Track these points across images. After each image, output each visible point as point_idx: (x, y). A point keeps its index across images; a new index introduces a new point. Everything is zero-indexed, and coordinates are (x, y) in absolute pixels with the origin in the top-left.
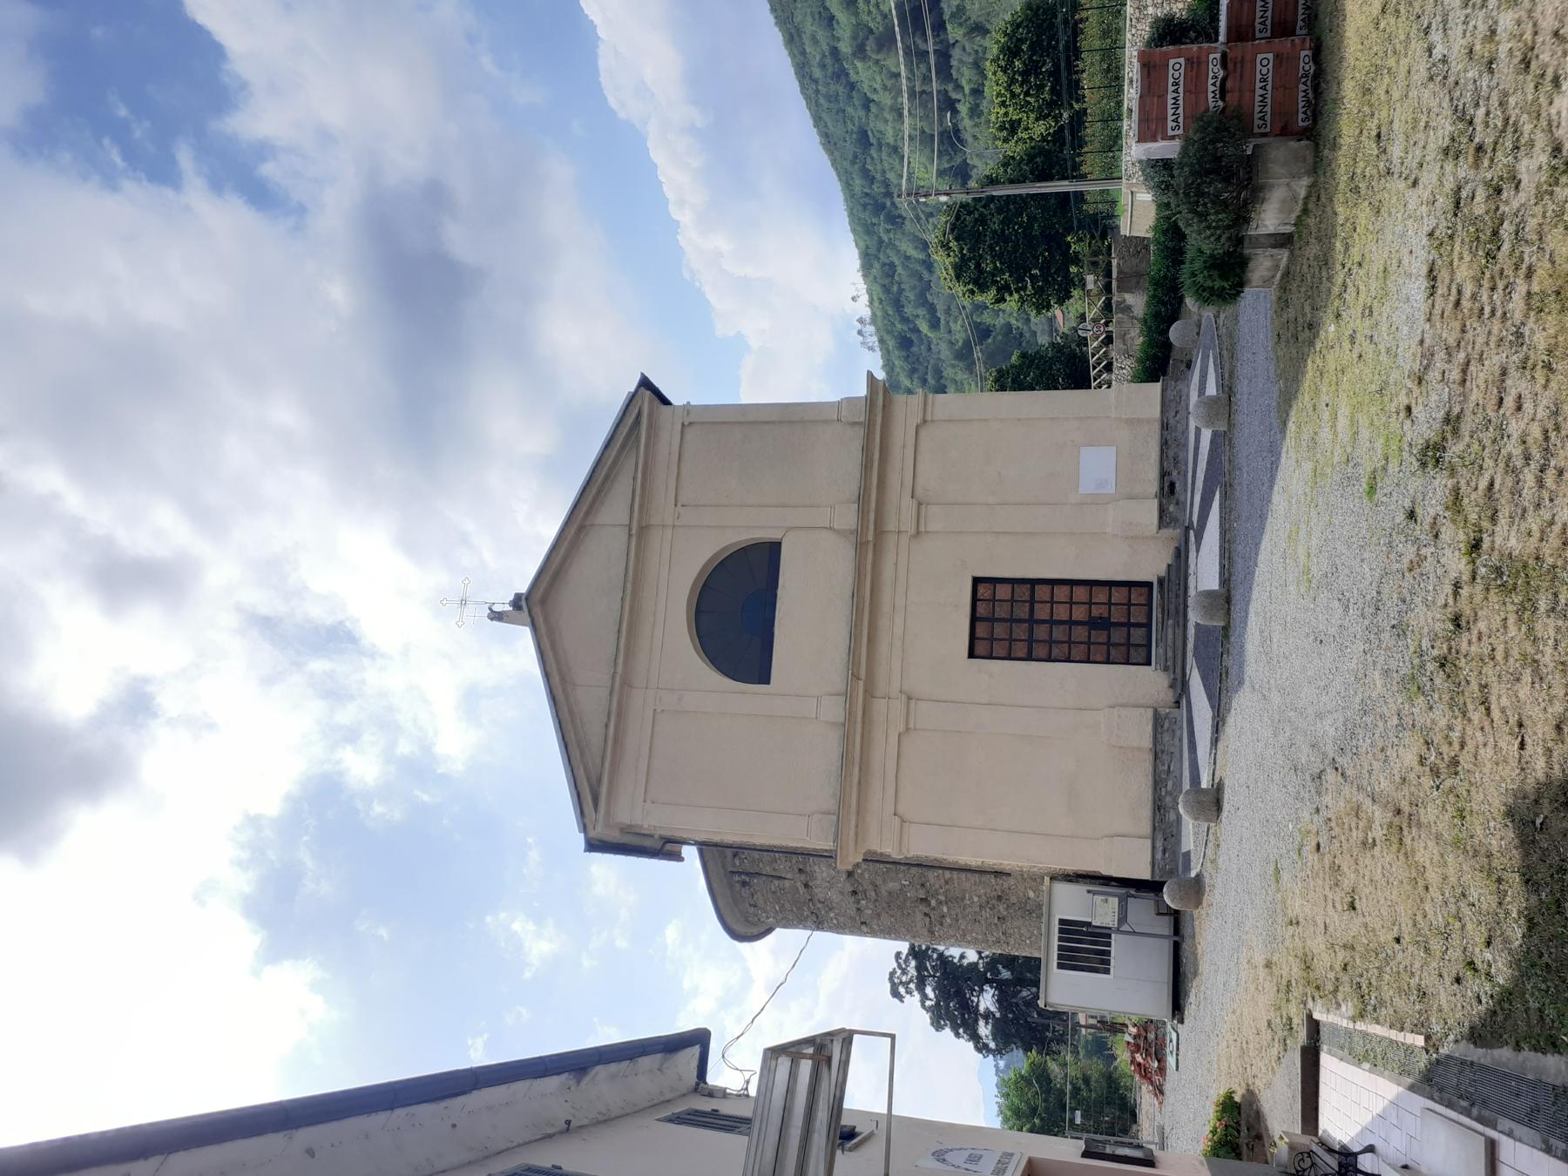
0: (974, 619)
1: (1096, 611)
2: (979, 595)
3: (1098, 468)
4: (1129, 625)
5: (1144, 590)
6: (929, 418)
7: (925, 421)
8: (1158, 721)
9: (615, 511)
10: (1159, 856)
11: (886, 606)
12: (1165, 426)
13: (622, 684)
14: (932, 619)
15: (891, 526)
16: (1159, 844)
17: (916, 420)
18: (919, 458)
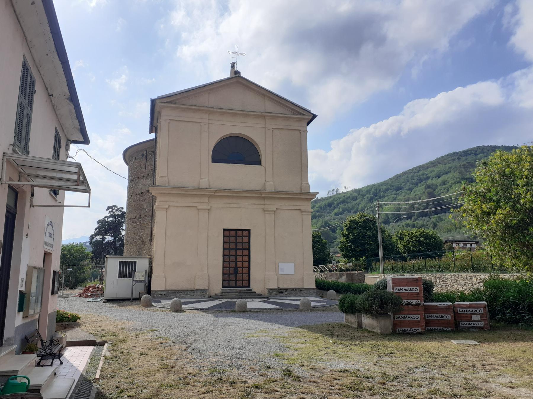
1: (240, 269)
2: (244, 232)
4: (236, 280)
5: (247, 284)
7: (302, 212)
8: (204, 291)
9: (270, 107)
10: (159, 293)
11: (240, 201)
12: (301, 290)
13: (211, 111)
14: (236, 217)
15: (267, 202)
16: (163, 293)
17: (303, 209)
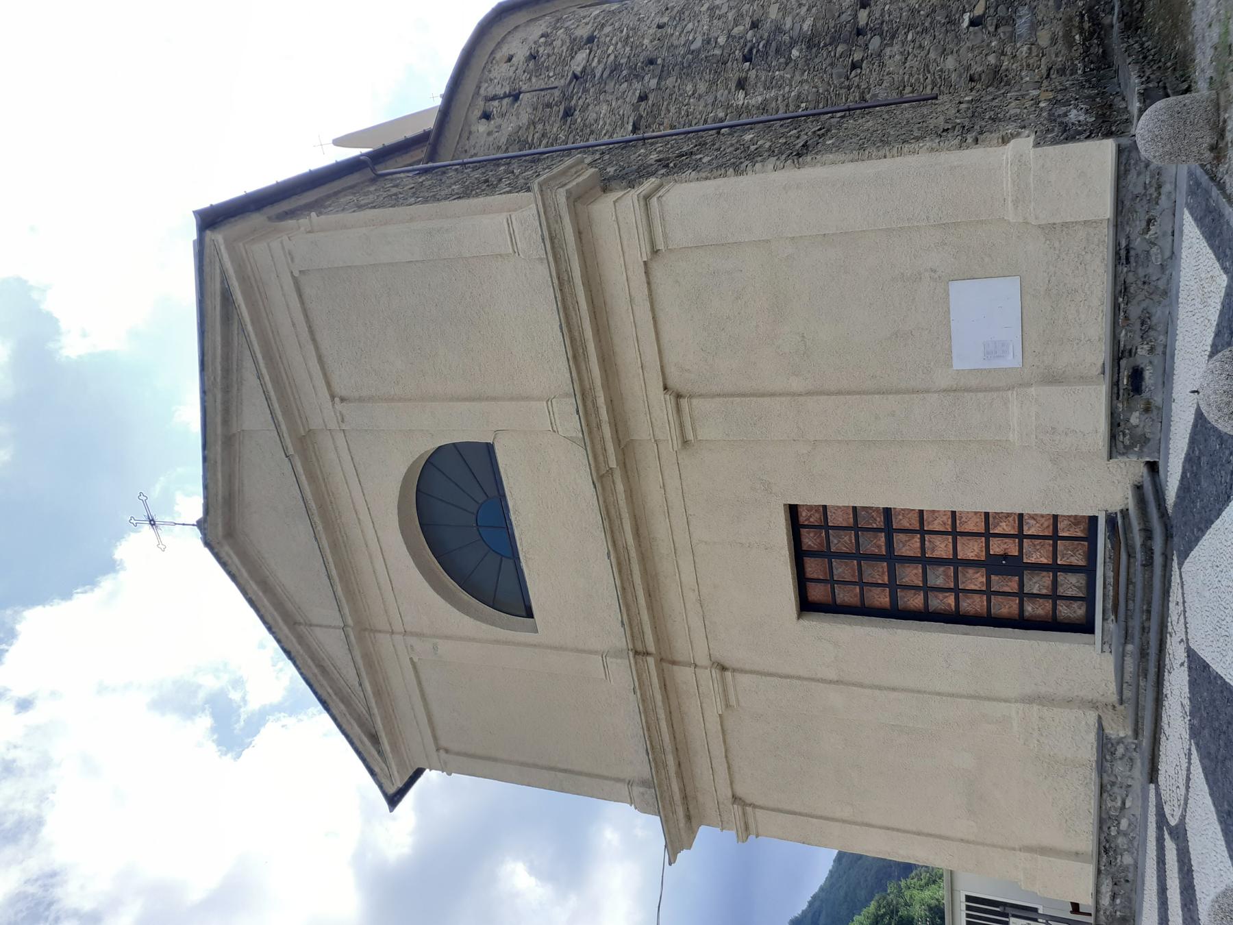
0: (799, 555)
1: (997, 547)
3: (985, 319)
6: (660, 246)
7: (655, 252)
9: (254, 416)
10: (1105, 901)
11: (663, 547)
12: (1123, 256)
13: (361, 631)
15: (641, 431)
17: (638, 252)
18: (662, 317)
